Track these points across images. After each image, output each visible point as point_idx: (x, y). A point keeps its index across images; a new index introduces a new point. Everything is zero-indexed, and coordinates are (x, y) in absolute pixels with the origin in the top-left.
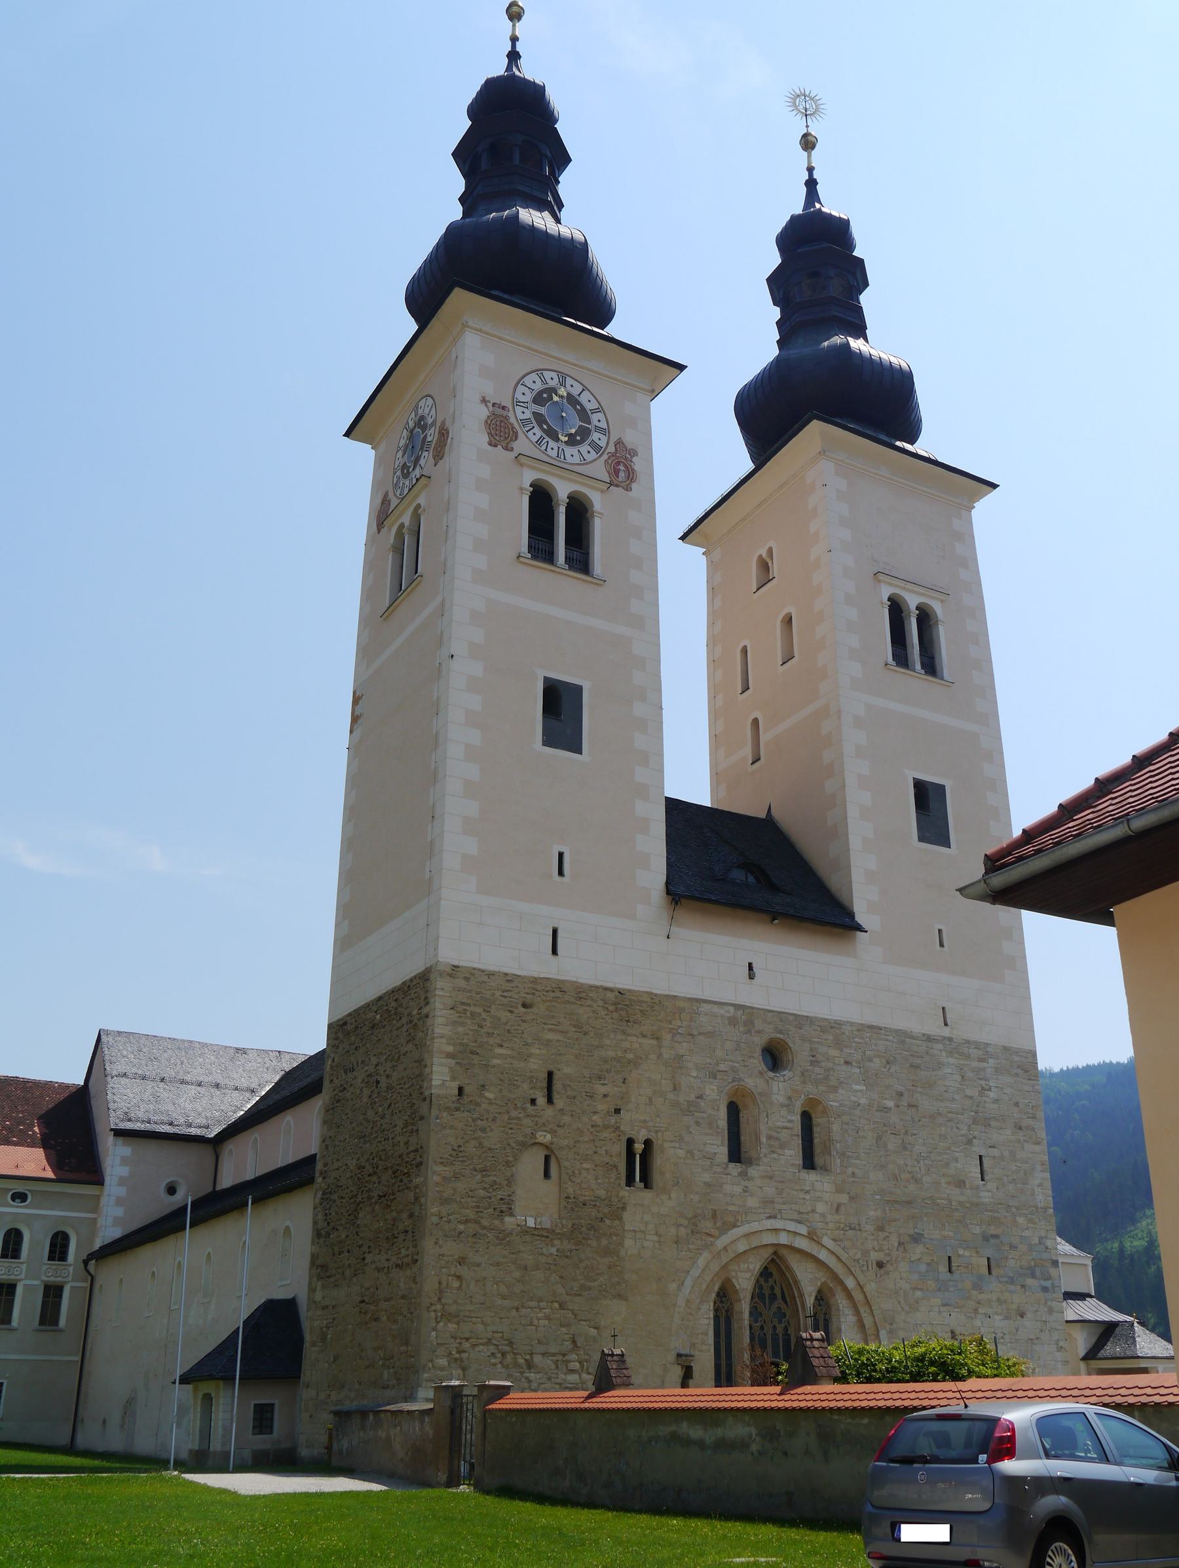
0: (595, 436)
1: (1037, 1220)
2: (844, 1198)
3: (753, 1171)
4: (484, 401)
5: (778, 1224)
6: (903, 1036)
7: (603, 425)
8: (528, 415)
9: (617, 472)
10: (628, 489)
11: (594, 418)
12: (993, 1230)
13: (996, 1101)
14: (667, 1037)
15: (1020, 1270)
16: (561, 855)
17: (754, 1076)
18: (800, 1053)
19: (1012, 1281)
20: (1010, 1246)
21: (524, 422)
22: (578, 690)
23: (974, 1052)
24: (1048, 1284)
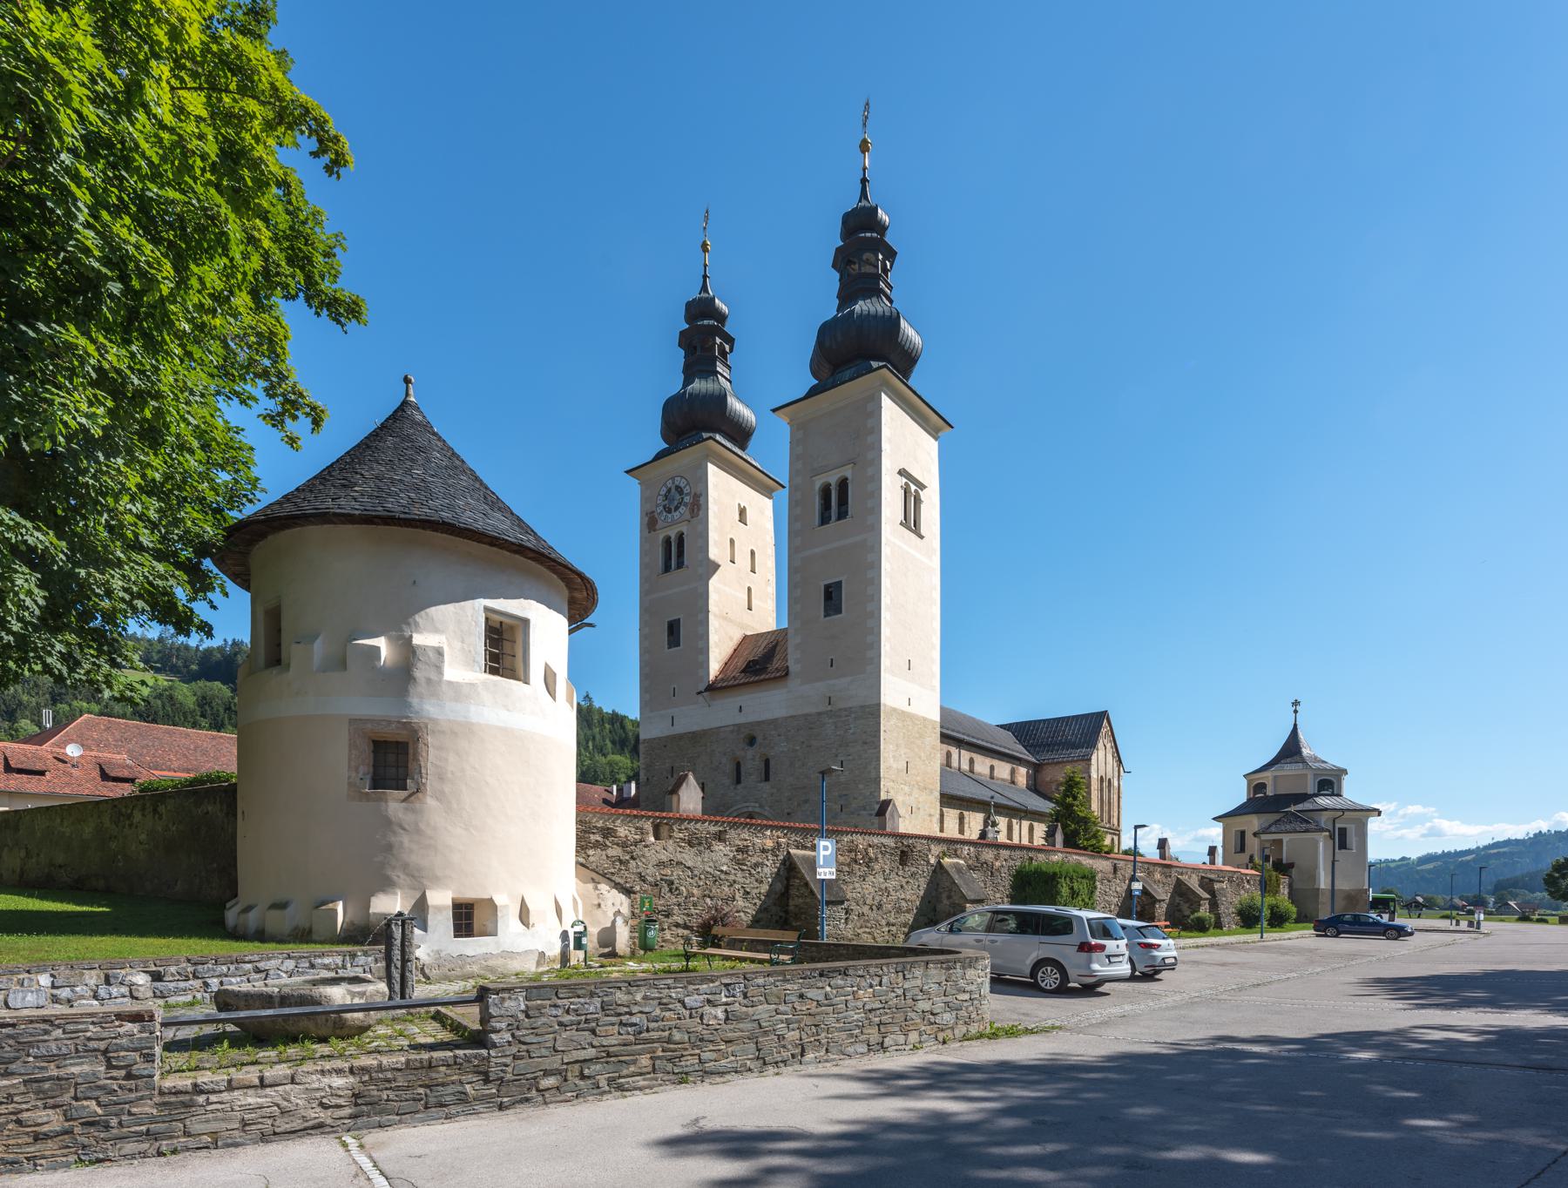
0: (687, 499)
2: (775, 790)
3: (739, 787)
5: (747, 804)
8: (661, 508)
10: (698, 515)
11: (685, 492)
12: (844, 793)
13: (853, 734)
19: (852, 813)
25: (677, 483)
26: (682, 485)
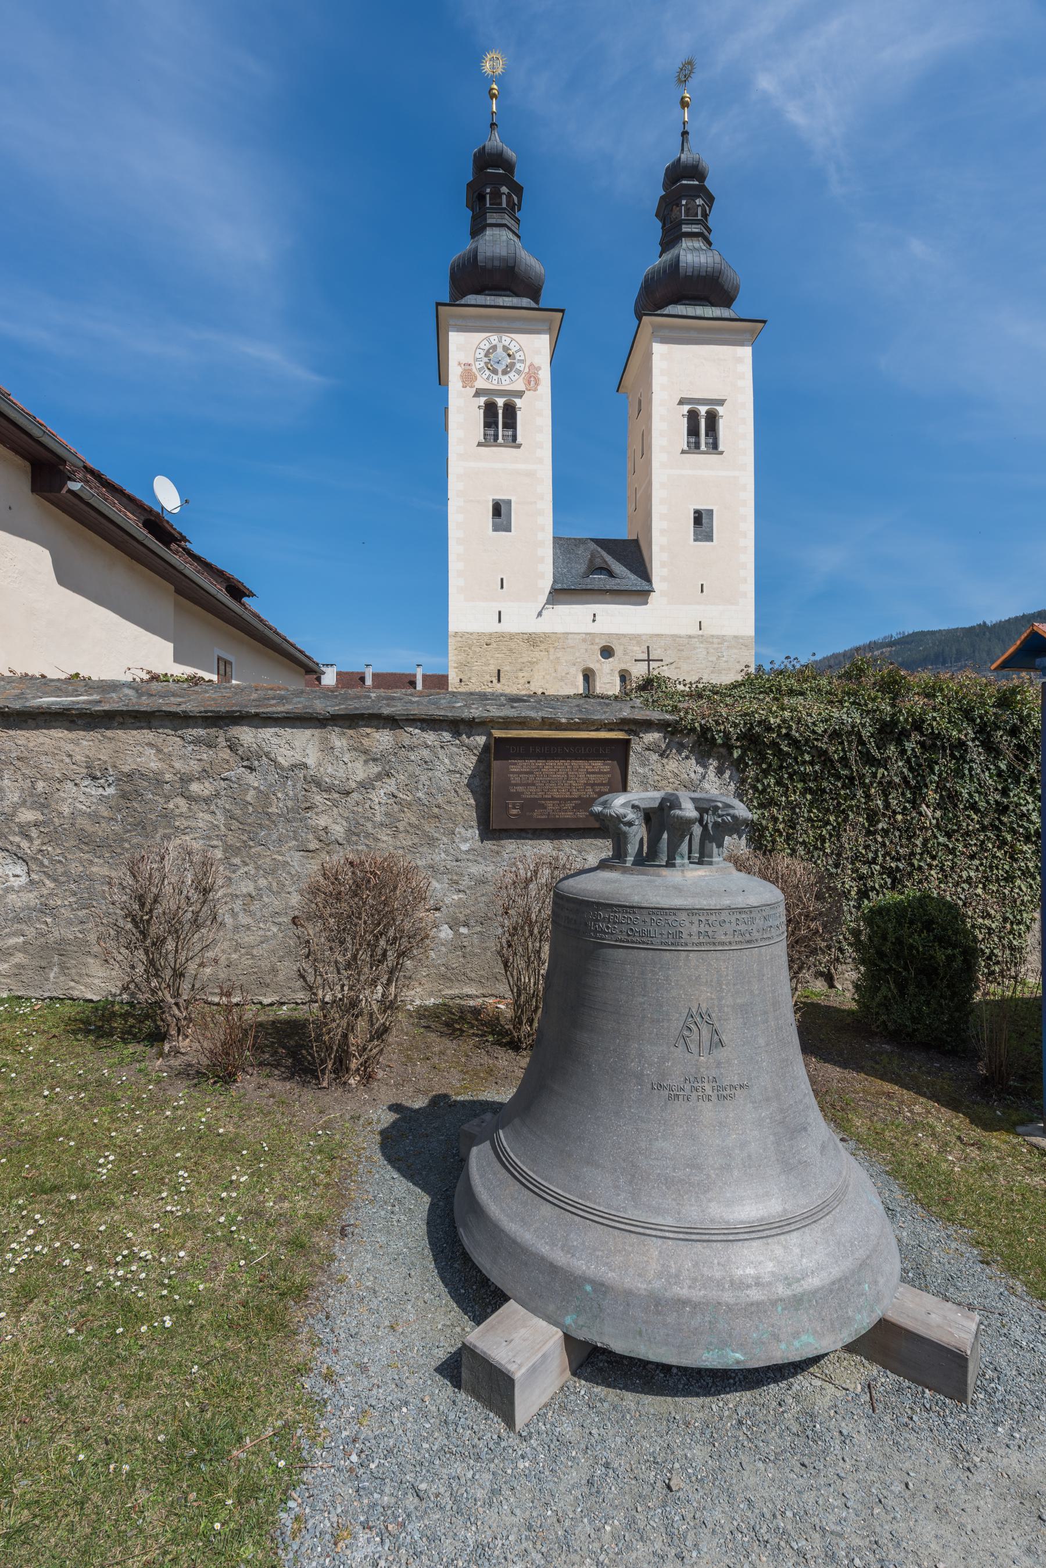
0: (518, 366)
4: (459, 364)
6: (674, 637)
7: (522, 358)
8: (482, 364)
9: (529, 383)
10: (536, 390)
11: (517, 356)
14: (552, 650)
16: (502, 580)
17: (596, 662)
18: (618, 650)
21: (480, 370)
22: (509, 503)
23: (715, 640)
25: (506, 344)
26: (513, 348)
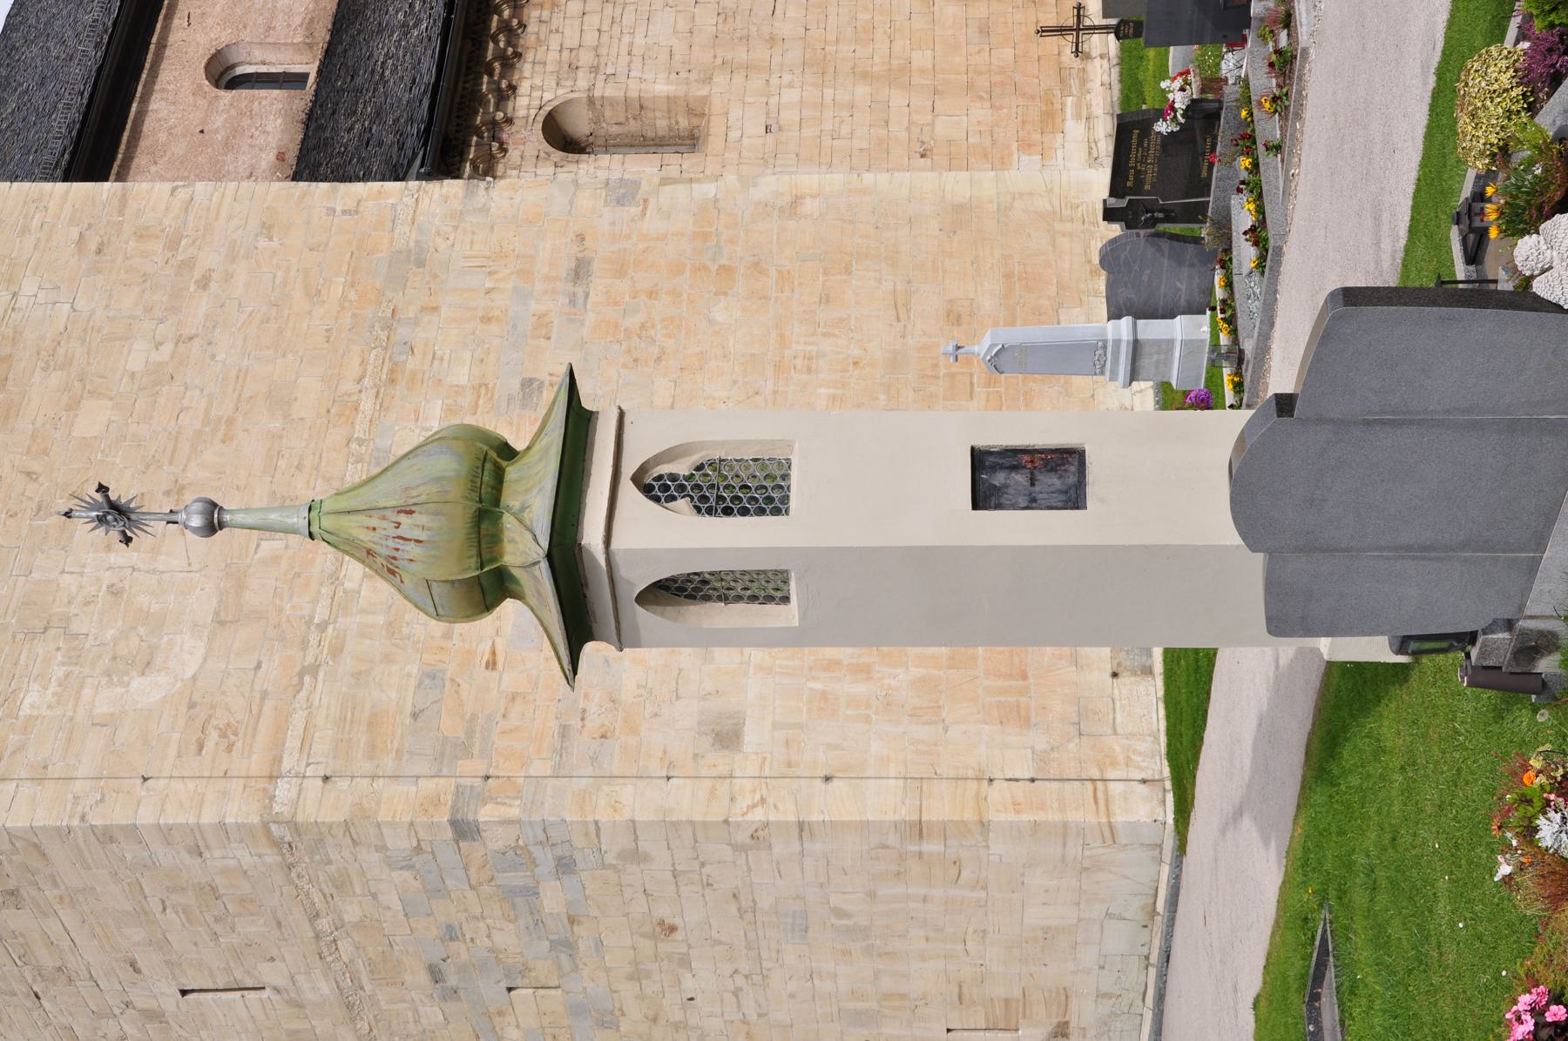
1: (332, 869)
15: (521, 922)
20: (451, 939)
24: (545, 858)
